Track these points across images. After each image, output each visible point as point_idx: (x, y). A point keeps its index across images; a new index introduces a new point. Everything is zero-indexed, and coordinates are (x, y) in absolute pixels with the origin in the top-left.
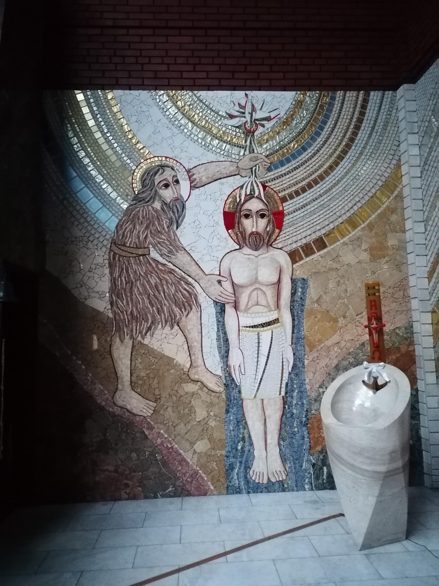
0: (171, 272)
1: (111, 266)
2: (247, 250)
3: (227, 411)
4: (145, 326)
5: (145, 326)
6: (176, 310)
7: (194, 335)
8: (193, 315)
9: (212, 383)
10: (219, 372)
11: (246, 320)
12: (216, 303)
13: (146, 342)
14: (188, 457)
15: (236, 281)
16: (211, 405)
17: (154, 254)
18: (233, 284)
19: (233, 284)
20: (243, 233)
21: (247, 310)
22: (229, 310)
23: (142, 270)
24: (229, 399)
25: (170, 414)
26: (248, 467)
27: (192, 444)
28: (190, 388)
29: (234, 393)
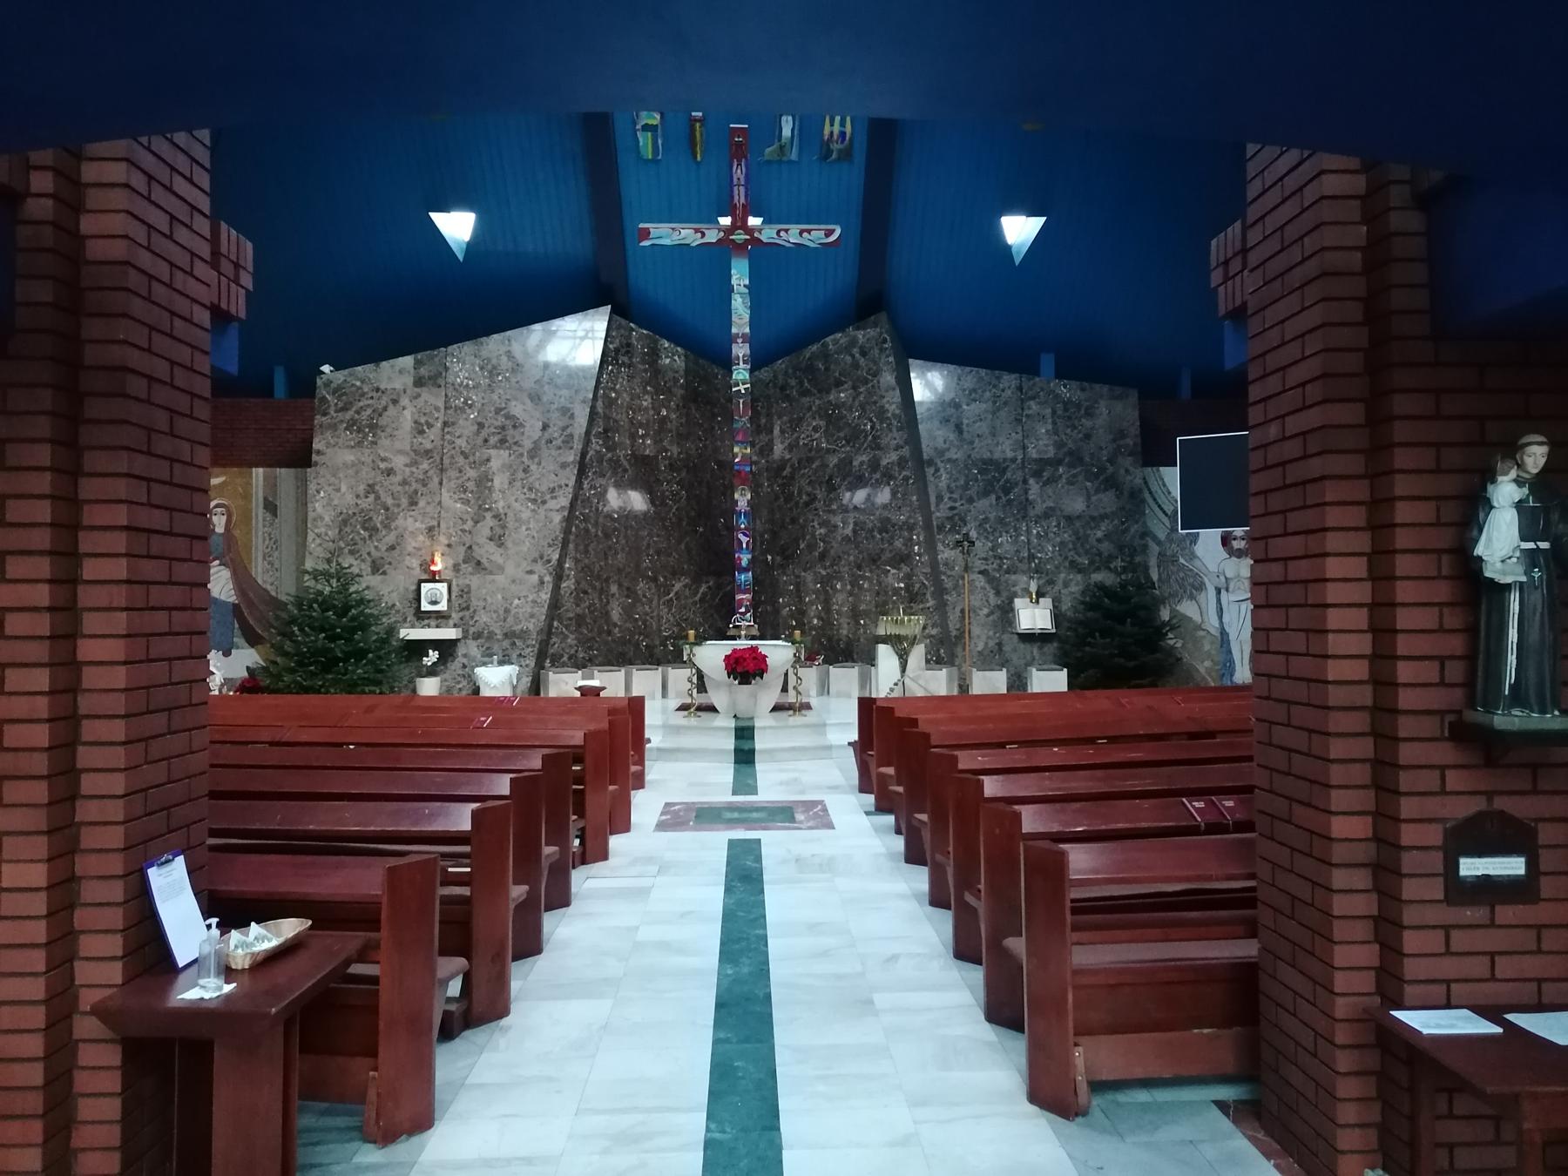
0: (1191, 570)
1: (1159, 567)
2: (1234, 559)
3: (1221, 646)
4: (1177, 600)
5: (1177, 600)
6: (1194, 592)
7: (1203, 605)
8: (1203, 594)
9: (1213, 631)
10: (1217, 625)
11: (1233, 598)
12: (1216, 588)
13: (1178, 608)
14: (1202, 670)
15: (1228, 576)
16: (1212, 643)
17: (1182, 560)
18: (1226, 578)
19: (1226, 578)
20: (1232, 547)
21: (1233, 591)
22: (1223, 592)
23: (1175, 569)
24: (1222, 640)
25: (1190, 646)
26: (1232, 676)
27: (1202, 662)
28: (1202, 633)
29: (1225, 637)
